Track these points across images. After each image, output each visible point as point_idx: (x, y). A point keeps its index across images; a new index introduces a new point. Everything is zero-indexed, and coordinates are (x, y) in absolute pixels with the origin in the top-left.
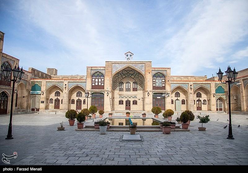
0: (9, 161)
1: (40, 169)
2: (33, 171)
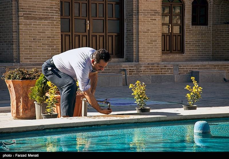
0: (8, 148)
1: (37, 156)
2: (31, 157)
